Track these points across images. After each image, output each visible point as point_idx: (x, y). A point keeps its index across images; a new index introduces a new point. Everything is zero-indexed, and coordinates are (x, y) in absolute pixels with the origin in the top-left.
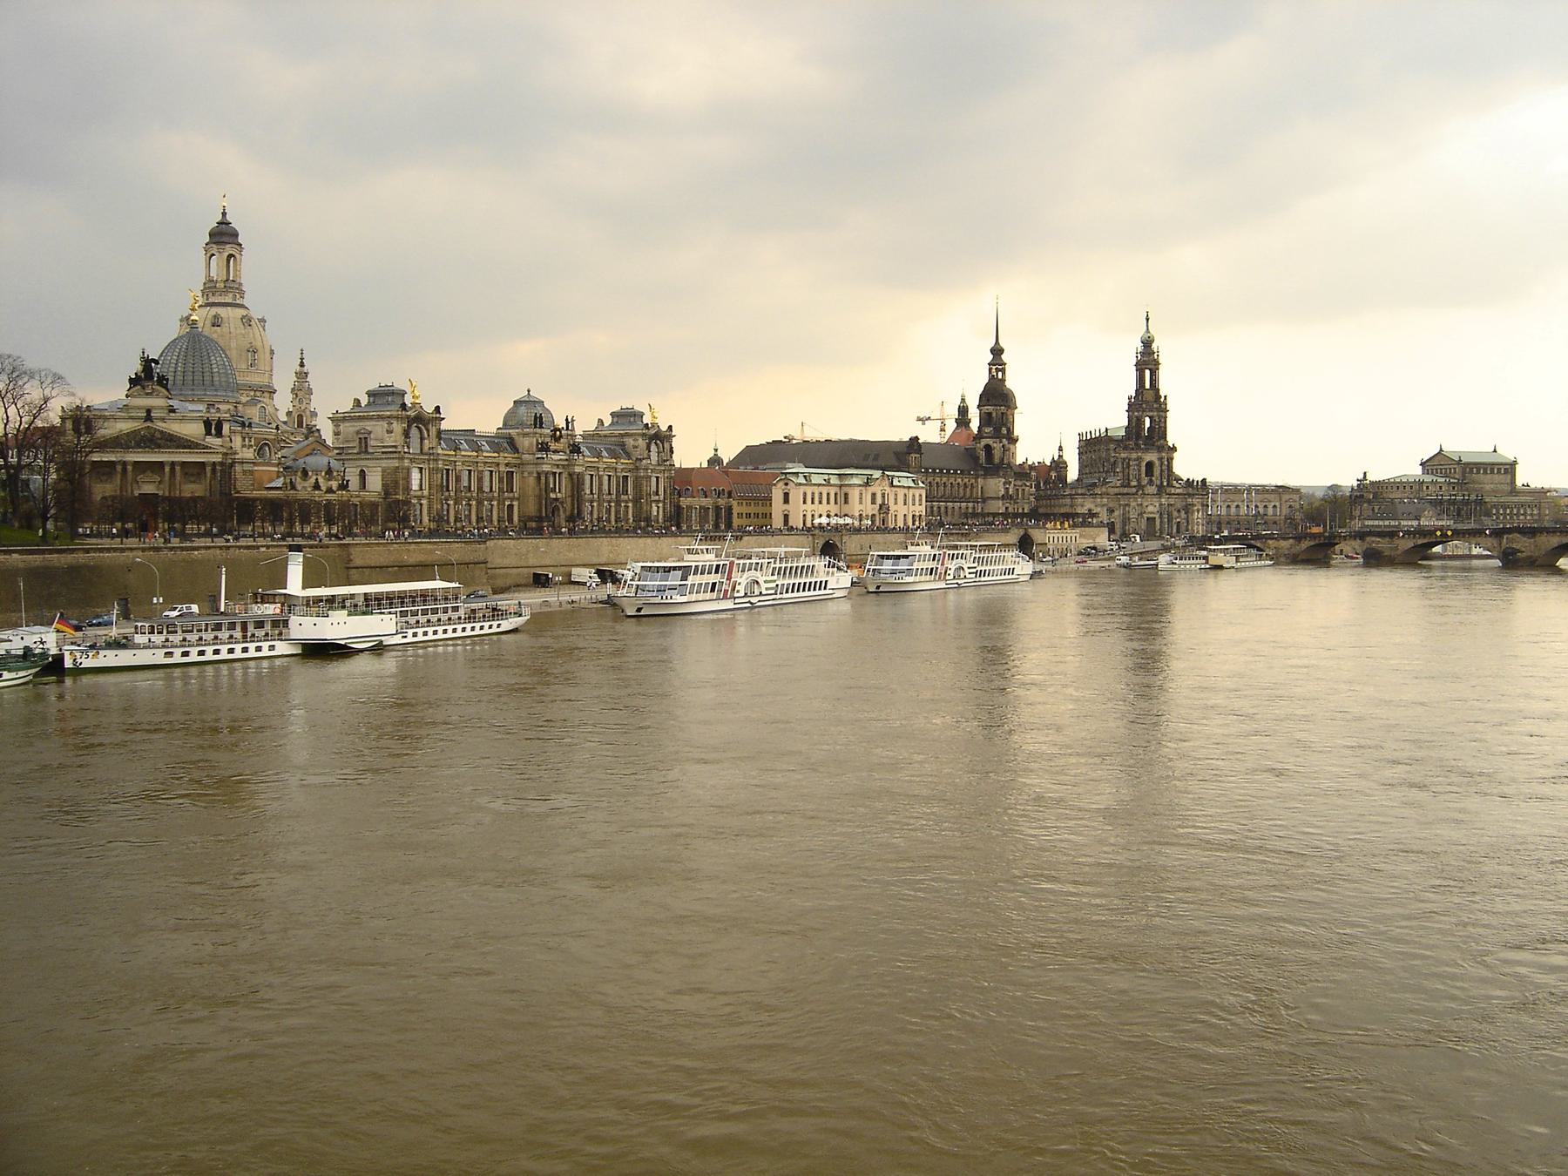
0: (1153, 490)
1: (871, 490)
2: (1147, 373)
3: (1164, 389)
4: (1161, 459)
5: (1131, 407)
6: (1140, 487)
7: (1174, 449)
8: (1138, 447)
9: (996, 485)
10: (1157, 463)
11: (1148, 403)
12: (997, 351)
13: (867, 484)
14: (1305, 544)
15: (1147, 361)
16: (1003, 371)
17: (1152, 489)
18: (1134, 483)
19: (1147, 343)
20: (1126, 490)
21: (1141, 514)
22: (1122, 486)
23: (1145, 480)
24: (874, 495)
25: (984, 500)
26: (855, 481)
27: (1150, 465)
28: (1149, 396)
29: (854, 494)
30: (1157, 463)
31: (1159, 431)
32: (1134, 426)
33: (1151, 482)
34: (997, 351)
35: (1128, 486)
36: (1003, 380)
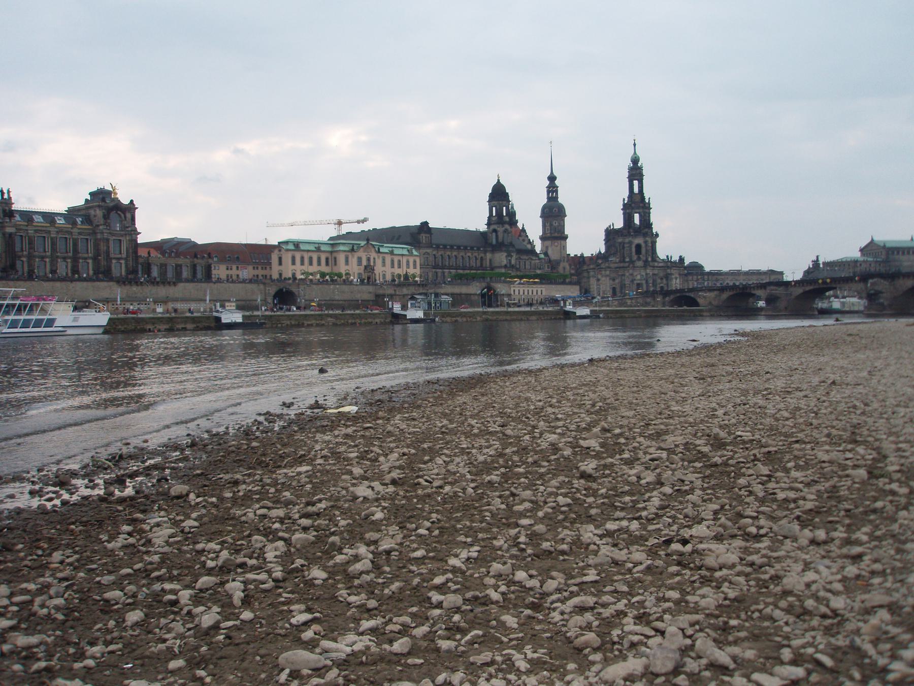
0: (640, 263)
1: (356, 255)
2: (636, 183)
3: (647, 194)
4: (646, 242)
5: (626, 207)
6: (631, 262)
7: (657, 235)
8: (629, 234)
9: (501, 258)
10: (643, 245)
11: (636, 204)
12: (552, 178)
13: (353, 250)
14: (725, 295)
15: (636, 172)
16: (557, 191)
17: (640, 263)
18: (627, 260)
19: (635, 160)
20: (622, 265)
21: (632, 281)
22: (620, 262)
23: (635, 257)
24: (360, 259)
25: (492, 269)
26: (342, 248)
27: (638, 247)
28: (638, 199)
29: (341, 258)
30: (643, 245)
31: (646, 224)
32: (628, 219)
33: (639, 259)
34: (552, 178)
35: (624, 261)
36: (557, 198)
